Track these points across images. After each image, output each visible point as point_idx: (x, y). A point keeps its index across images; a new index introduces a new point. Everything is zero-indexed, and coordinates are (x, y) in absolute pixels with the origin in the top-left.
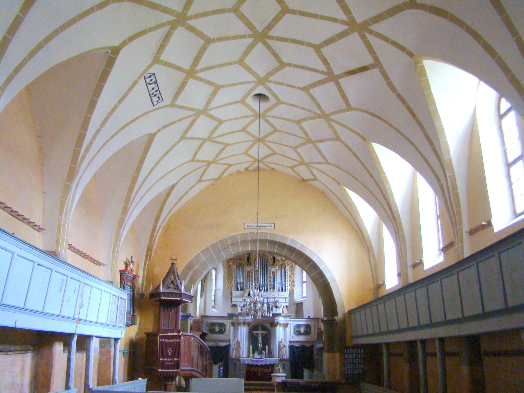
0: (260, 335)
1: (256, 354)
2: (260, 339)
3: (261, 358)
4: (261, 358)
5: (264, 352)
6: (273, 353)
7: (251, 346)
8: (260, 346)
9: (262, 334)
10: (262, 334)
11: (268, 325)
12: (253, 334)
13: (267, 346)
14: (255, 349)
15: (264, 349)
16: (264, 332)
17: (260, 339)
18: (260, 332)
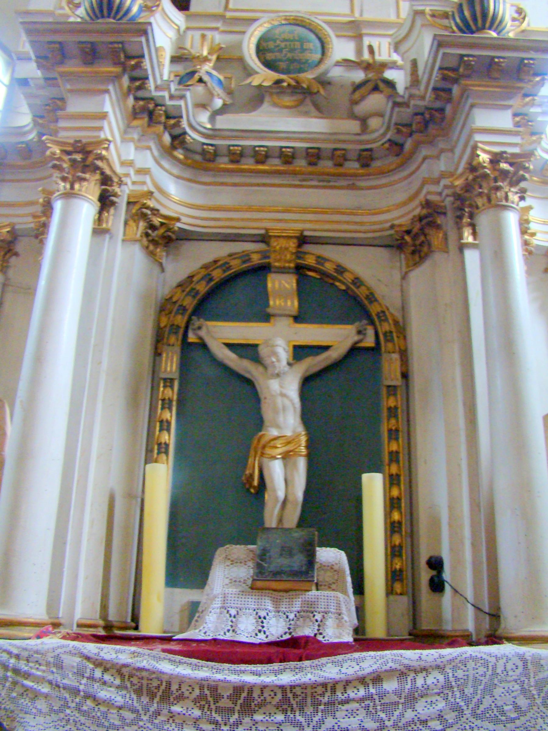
0: (283, 353)
1: (228, 573)
2: (283, 397)
3: (294, 649)
4: (294, 649)
5: (330, 556)
6: (461, 573)
7: (160, 480)
8: (285, 480)
9: (300, 352)
10: (300, 352)
11: (371, 269)
12: (194, 351)
13: (373, 486)
14: (213, 517)
15: (330, 513)
16: (338, 337)
17: (283, 397)
18: (278, 339)
